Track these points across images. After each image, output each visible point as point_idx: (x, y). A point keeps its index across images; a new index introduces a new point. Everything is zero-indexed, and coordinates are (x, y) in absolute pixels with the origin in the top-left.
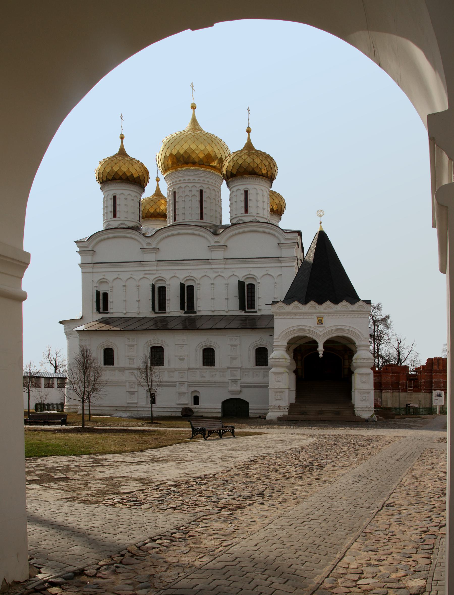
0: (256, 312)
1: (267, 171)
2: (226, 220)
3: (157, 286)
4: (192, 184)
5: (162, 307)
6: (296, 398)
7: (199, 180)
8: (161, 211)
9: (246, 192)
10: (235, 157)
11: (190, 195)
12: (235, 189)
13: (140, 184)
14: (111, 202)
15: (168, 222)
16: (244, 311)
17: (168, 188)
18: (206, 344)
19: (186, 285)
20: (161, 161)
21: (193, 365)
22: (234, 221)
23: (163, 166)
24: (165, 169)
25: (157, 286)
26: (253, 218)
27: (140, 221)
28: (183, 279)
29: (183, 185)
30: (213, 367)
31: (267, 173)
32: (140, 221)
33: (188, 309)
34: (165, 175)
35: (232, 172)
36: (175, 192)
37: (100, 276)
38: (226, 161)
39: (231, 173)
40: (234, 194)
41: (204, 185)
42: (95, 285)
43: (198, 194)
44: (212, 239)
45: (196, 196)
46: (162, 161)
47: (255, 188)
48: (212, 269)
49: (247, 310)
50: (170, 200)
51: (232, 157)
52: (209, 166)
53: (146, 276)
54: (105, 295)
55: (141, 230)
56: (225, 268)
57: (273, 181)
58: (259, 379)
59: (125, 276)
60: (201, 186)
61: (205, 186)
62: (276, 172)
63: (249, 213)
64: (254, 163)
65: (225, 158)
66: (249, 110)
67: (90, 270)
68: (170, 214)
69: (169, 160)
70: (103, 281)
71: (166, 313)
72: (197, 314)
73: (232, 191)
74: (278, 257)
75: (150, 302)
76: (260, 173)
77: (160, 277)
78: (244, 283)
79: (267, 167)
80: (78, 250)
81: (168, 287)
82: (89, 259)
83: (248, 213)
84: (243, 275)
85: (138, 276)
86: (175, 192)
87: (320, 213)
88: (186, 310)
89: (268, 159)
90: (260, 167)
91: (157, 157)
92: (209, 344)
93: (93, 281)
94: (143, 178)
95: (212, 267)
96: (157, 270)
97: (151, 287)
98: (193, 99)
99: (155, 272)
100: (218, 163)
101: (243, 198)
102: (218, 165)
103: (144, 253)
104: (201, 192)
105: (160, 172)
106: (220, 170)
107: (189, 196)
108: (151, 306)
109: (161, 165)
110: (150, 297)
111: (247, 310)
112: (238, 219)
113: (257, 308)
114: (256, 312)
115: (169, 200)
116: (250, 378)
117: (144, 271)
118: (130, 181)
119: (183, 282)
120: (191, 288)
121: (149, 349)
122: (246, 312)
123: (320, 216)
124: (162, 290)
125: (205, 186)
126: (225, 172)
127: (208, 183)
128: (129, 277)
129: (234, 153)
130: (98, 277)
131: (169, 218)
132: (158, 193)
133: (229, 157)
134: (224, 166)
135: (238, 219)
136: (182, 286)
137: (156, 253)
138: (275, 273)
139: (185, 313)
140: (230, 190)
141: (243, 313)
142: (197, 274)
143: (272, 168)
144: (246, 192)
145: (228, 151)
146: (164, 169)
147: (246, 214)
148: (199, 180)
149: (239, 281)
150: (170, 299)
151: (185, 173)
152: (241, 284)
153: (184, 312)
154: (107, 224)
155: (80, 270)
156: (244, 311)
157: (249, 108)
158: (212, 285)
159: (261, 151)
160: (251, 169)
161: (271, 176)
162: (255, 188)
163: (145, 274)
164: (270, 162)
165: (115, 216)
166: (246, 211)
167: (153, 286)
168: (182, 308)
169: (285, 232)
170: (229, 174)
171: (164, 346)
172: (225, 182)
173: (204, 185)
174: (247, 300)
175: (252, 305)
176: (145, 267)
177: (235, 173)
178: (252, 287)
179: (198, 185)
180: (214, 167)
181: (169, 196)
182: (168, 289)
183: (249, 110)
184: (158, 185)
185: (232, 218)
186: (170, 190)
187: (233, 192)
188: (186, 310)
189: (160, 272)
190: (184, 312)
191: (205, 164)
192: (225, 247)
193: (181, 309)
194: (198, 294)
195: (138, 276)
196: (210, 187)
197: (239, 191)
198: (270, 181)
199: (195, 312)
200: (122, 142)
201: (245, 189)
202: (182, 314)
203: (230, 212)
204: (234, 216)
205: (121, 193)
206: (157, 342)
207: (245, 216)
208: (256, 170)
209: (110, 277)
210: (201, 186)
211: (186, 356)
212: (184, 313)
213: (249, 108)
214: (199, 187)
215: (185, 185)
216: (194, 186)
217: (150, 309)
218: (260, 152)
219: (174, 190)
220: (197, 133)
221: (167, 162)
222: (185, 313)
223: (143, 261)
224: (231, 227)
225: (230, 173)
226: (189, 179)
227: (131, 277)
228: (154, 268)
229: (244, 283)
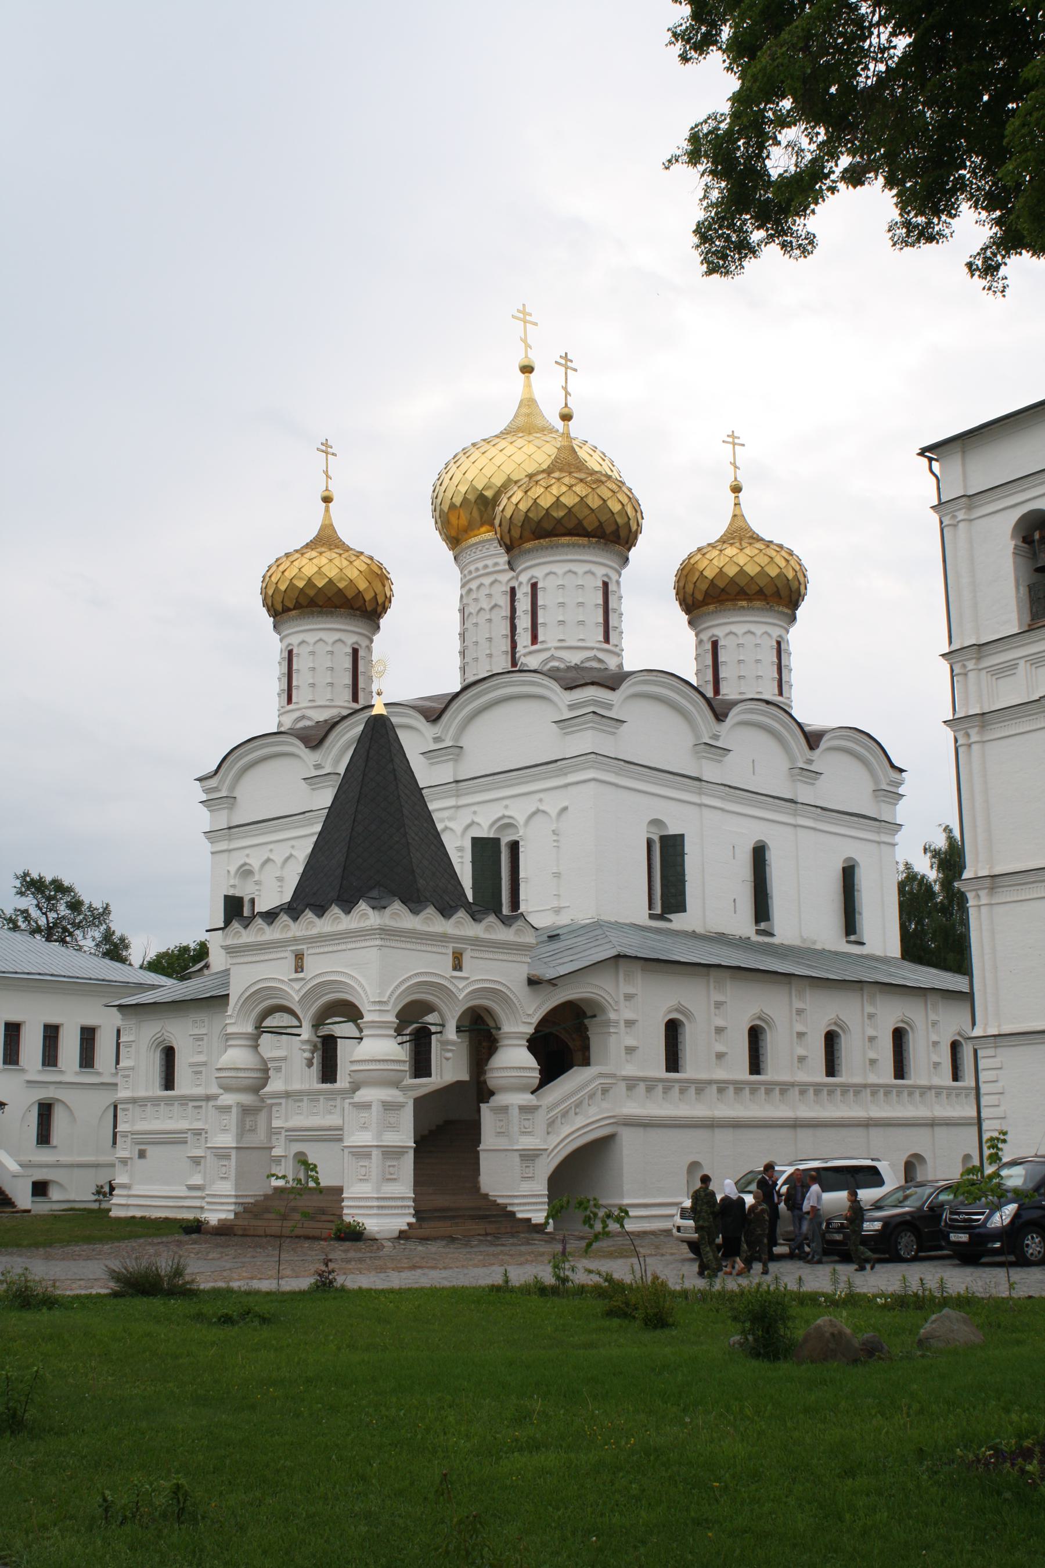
37: (238, 859)
42: (232, 882)
56: (458, 807)
74: (556, 761)
84: (490, 822)
90: (555, 514)
93: (228, 871)
130: (238, 860)
138: (552, 804)
147: (535, 647)
165: (290, 700)
192: (457, 750)
200: (327, 510)
205: (300, 640)
207: (530, 653)
223: (312, 811)
224: (460, 697)
229: (498, 840)
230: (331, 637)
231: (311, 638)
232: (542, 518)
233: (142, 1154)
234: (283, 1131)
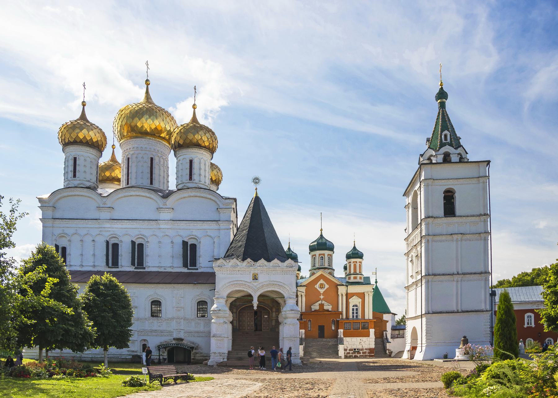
0: (197, 269)
1: (210, 144)
2: (172, 186)
3: (111, 243)
5: (115, 263)
6: (232, 346)
8: (115, 175)
10: (183, 129)
12: (181, 158)
13: (98, 148)
14: (71, 162)
15: (121, 185)
16: (187, 268)
17: (123, 154)
20: (117, 129)
22: (180, 187)
23: (119, 134)
24: (122, 136)
25: (111, 243)
26: (197, 185)
27: (97, 183)
31: (209, 145)
32: (97, 183)
33: (137, 266)
34: (121, 142)
35: (180, 142)
36: (128, 159)
38: (175, 132)
39: (179, 143)
40: (181, 162)
44: (160, 201)
46: (119, 129)
49: (189, 267)
50: (124, 165)
51: (179, 129)
52: (160, 137)
55: (97, 190)
57: (213, 153)
58: (201, 328)
61: (154, 153)
62: (216, 145)
63: (192, 180)
64: (198, 136)
65: (174, 130)
66: (195, 89)
68: (123, 179)
69: (125, 128)
71: (118, 268)
72: (147, 270)
73: (178, 160)
75: (105, 258)
76: (203, 144)
78: (188, 242)
79: (209, 140)
83: (191, 180)
86: (128, 159)
88: (136, 265)
89: (210, 133)
91: (114, 125)
94: (101, 143)
97: (105, 244)
98: (148, 76)
100: (167, 134)
102: (167, 136)
105: (115, 139)
106: (169, 141)
108: (105, 260)
109: (118, 133)
110: (105, 253)
111: (189, 267)
112: (183, 185)
113: (198, 265)
114: (197, 269)
115: (124, 166)
116: (192, 327)
118: (89, 144)
119: (134, 240)
120: (141, 246)
122: (188, 269)
124: (116, 246)
126: (173, 142)
129: (182, 125)
131: (123, 181)
132: (113, 159)
133: (177, 129)
134: (172, 137)
135: (183, 185)
136: (133, 243)
139: (135, 269)
140: (177, 159)
141: (185, 270)
142: (147, 233)
143: (213, 141)
145: (176, 125)
146: (120, 136)
149: (183, 241)
150: (122, 255)
152: (185, 243)
153: (134, 267)
154: (67, 183)
156: (187, 268)
157: (195, 87)
159: (204, 126)
160: (195, 141)
161: (213, 148)
164: (212, 135)
166: (191, 178)
167: (107, 243)
168: (133, 264)
169: (223, 199)
170: (177, 144)
172: (172, 152)
174: (190, 258)
175: (194, 263)
178: (194, 247)
180: (164, 138)
181: (123, 162)
183: (195, 89)
184: (113, 151)
185: (178, 184)
186: (124, 156)
187: (179, 160)
188: (136, 265)
190: (134, 267)
191: (156, 135)
192: (172, 210)
193: (132, 265)
197: (185, 159)
198: (211, 153)
199: (144, 268)
202: (132, 269)
203: (176, 179)
204: (180, 182)
208: (200, 142)
212: (135, 269)
213: (195, 87)
217: (105, 264)
218: (204, 126)
219: (128, 157)
220: (150, 106)
221: (123, 131)
222: (136, 268)
225: (177, 144)
229: (188, 242)
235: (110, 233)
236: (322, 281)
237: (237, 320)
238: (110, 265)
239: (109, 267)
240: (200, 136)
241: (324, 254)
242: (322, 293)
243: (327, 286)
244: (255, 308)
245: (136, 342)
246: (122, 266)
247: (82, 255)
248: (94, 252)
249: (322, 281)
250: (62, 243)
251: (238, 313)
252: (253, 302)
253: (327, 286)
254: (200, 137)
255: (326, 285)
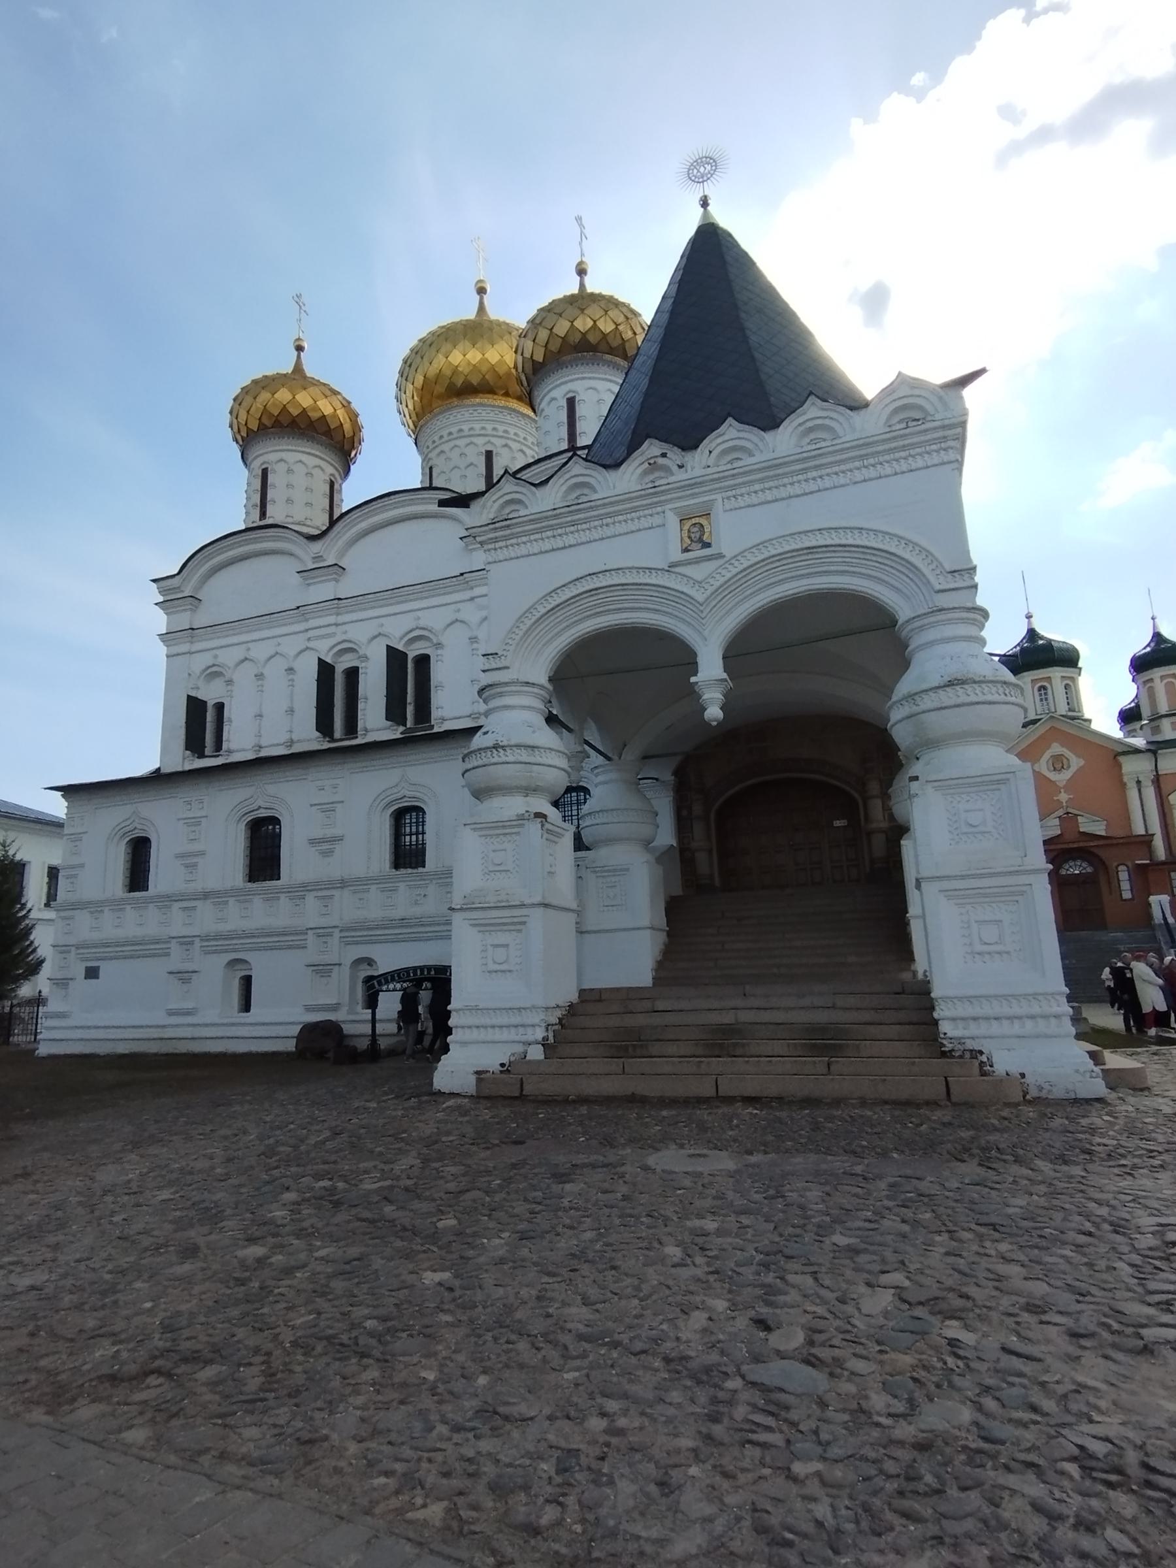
4: (468, 440)
7: (483, 428)
9: (571, 403)
11: (462, 466)
18: (399, 795)
19: (411, 655)
21: (359, 870)
28: (401, 639)
29: (446, 447)
30: (421, 870)
41: (493, 440)
43: (481, 462)
45: (476, 466)
47: (591, 388)
48: (472, 599)
53: (311, 644)
54: (220, 707)
59: (260, 652)
60: (489, 442)
61: (498, 442)
67: (184, 648)
70: (213, 673)
77: (345, 641)
80: (161, 599)
81: (363, 664)
82: (184, 620)
85: (291, 646)
87: (702, 169)
92: (407, 794)
95: (473, 595)
96: (337, 625)
99: (332, 629)
101: (563, 416)
103: (309, 585)
104: (489, 455)
107: (459, 468)
117: (307, 630)
119: (400, 647)
120: (423, 662)
121: (242, 826)
123: (702, 179)
124: (352, 675)
125: (498, 442)
127: (505, 435)
128: (272, 652)
136: (395, 658)
137: (337, 581)
142: (434, 619)
144: (571, 403)
148: (483, 428)
150: (366, 698)
151: (452, 418)
155: (162, 650)
158: (472, 643)
162: (591, 388)
163: (309, 639)
171: (281, 814)
173: (493, 440)
176: (311, 621)
177: (541, 360)
179: (480, 441)
182: (364, 670)
189: (345, 627)
193: (388, 717)
194: (439, 673)
195: (291, 646)
196: (510, 443)
201: (567, 393)
206: (263, 805)
209: (229, 657)
210: (489, 442)
211: (340, 839)
214: (482, 444)
215: (452, 444)
216: (471, 443)
219: (429, 465)
226: (461, 430)
227: (277, 653)
228: (332, 619)
230: (312, 461)
231: (291, 457)
232: (589, 330)
233: (92, 973)
234: (337, 931)
235: (333, 641)
236: (1056, 749)
237: (710, 851)
238: (338, 733)
239: (333, 740)
240: (589, 319)
241: (1049, 679)
242: (1061, 784)
243: (1076, 763)
244: (714, 713)
245: (336, 968)
246: (366, 730)
247: (261, 716)
248: (292, 701)
249: (1056, 749)
250: (210, 694)
251: (712, 816)
252: (693, 679)
253: (1076, 763)
254: (590, 323)
255: (1073, 756)
